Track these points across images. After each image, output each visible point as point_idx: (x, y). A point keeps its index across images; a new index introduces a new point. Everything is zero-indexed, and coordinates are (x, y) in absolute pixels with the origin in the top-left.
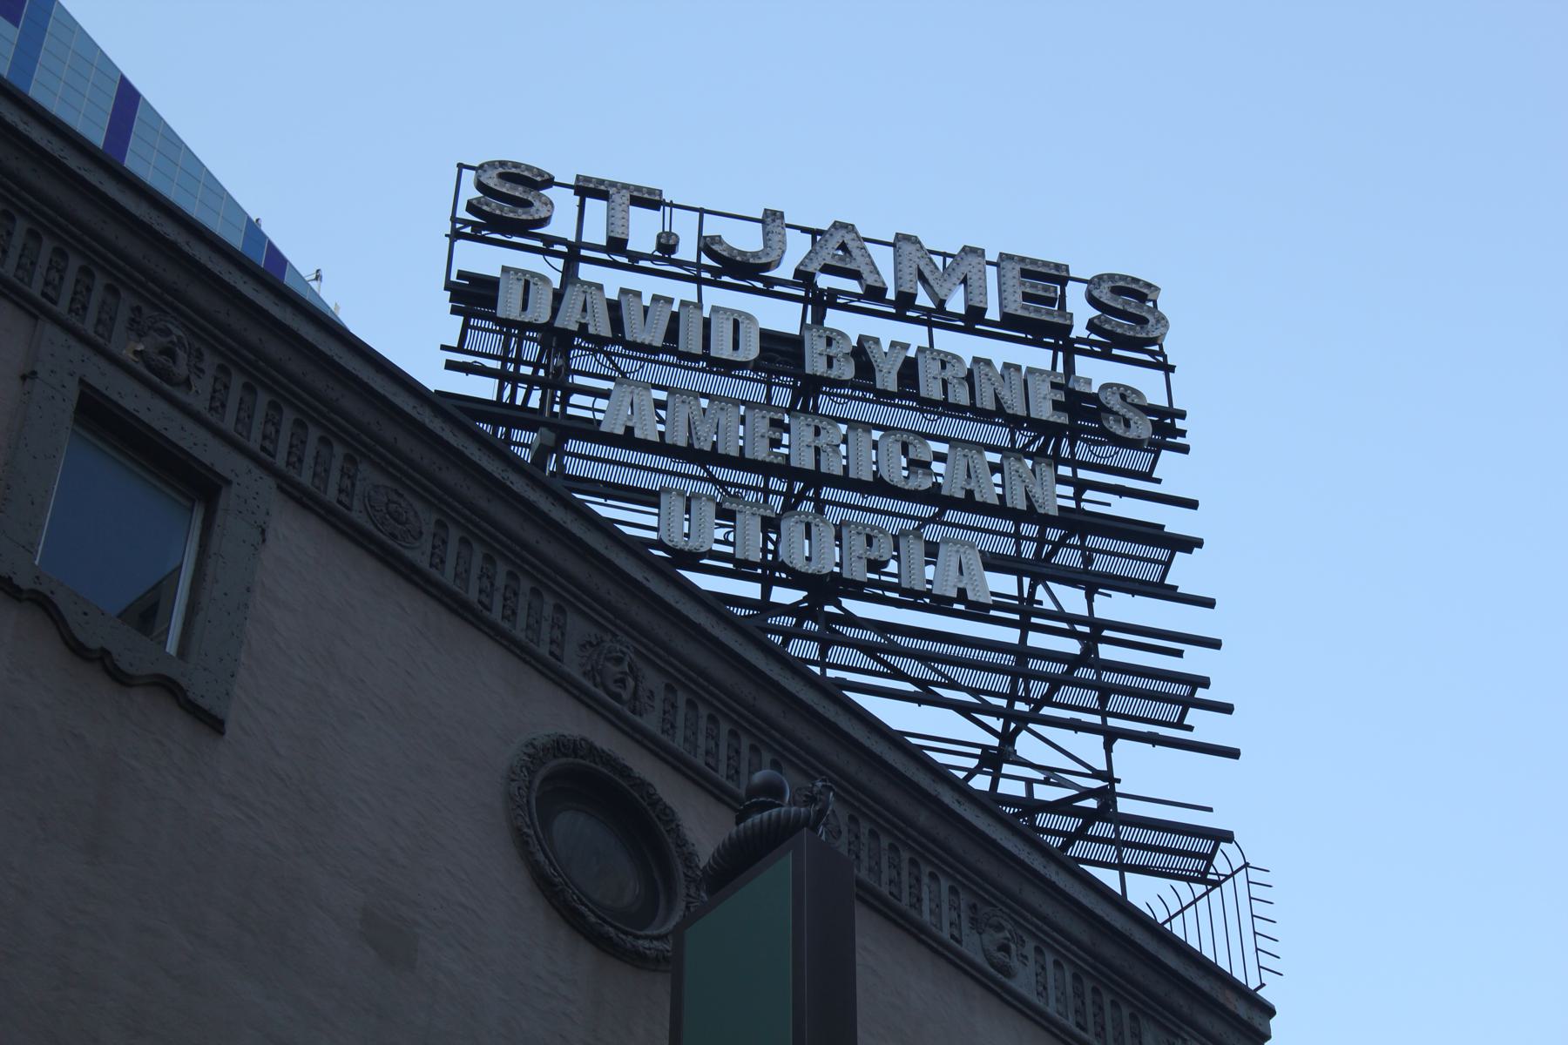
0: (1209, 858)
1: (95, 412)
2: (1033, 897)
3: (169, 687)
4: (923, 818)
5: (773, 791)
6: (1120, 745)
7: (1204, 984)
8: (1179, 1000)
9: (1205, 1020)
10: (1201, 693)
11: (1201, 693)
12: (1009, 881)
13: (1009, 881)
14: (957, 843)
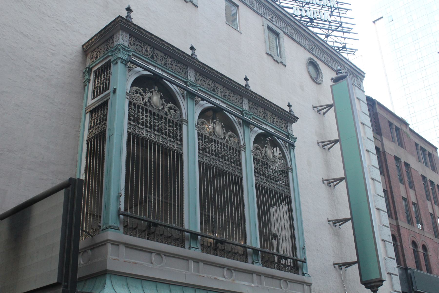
0: (354, 52)
1: (269, 29)
2: (346, 65)
3: (282, 63)
4: (336, 58)
5: (340, 70)
6: (346, 39)
7: (360, 72)
8: (358, 74)
9: (360, 76)
10: (352, 31)
11: (352, 31)
12: (344, 64)
13: (344, 64)
14: (339, 60)
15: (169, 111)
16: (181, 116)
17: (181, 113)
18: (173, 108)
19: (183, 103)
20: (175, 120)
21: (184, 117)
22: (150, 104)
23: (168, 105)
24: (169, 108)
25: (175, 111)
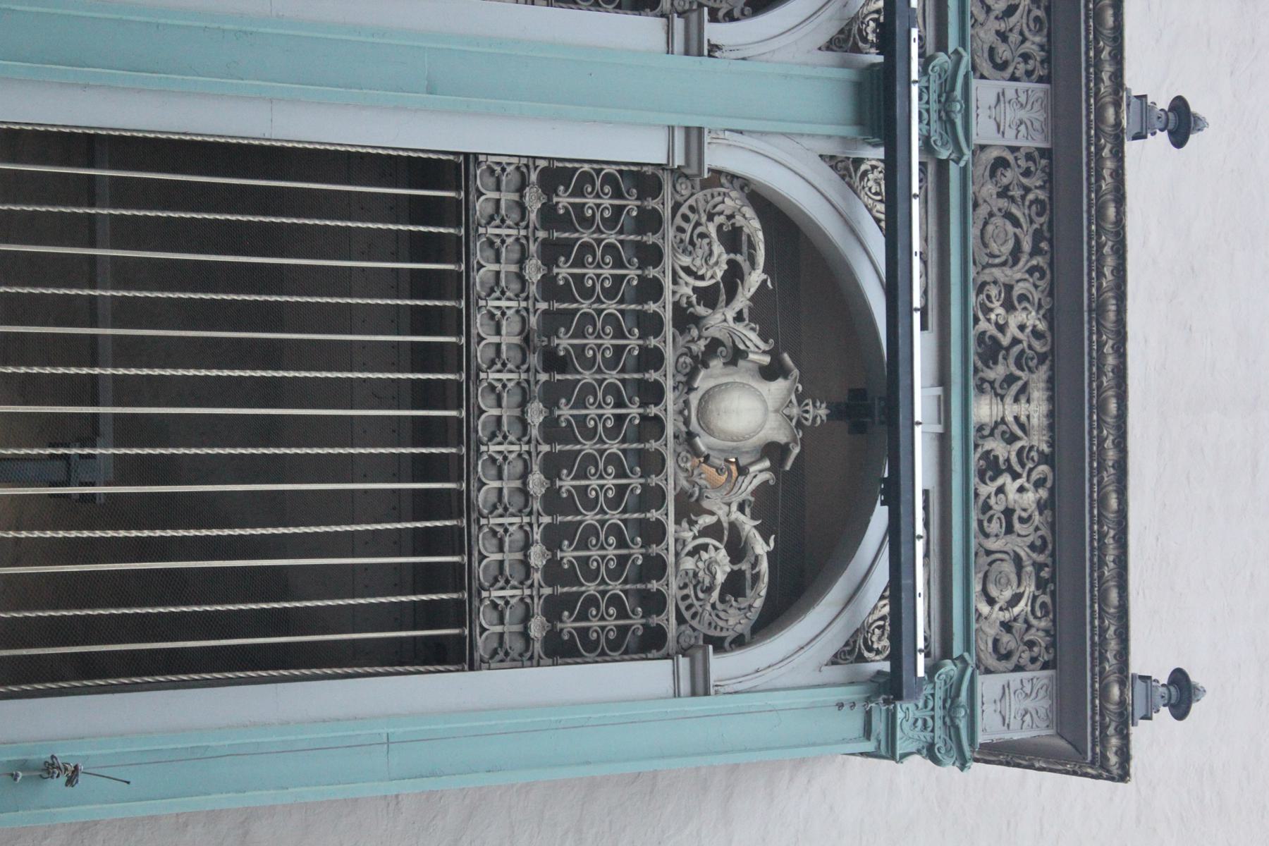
15: (714, 531)
16: (719, 645)
17: (740, 642)
18: (745, 566)
19: (816, 627)
20: (672, 587)
21: (721, 666)
22: (701, 362)
23: (748, 525)
24: (734, 527)
25: (735, 586)
